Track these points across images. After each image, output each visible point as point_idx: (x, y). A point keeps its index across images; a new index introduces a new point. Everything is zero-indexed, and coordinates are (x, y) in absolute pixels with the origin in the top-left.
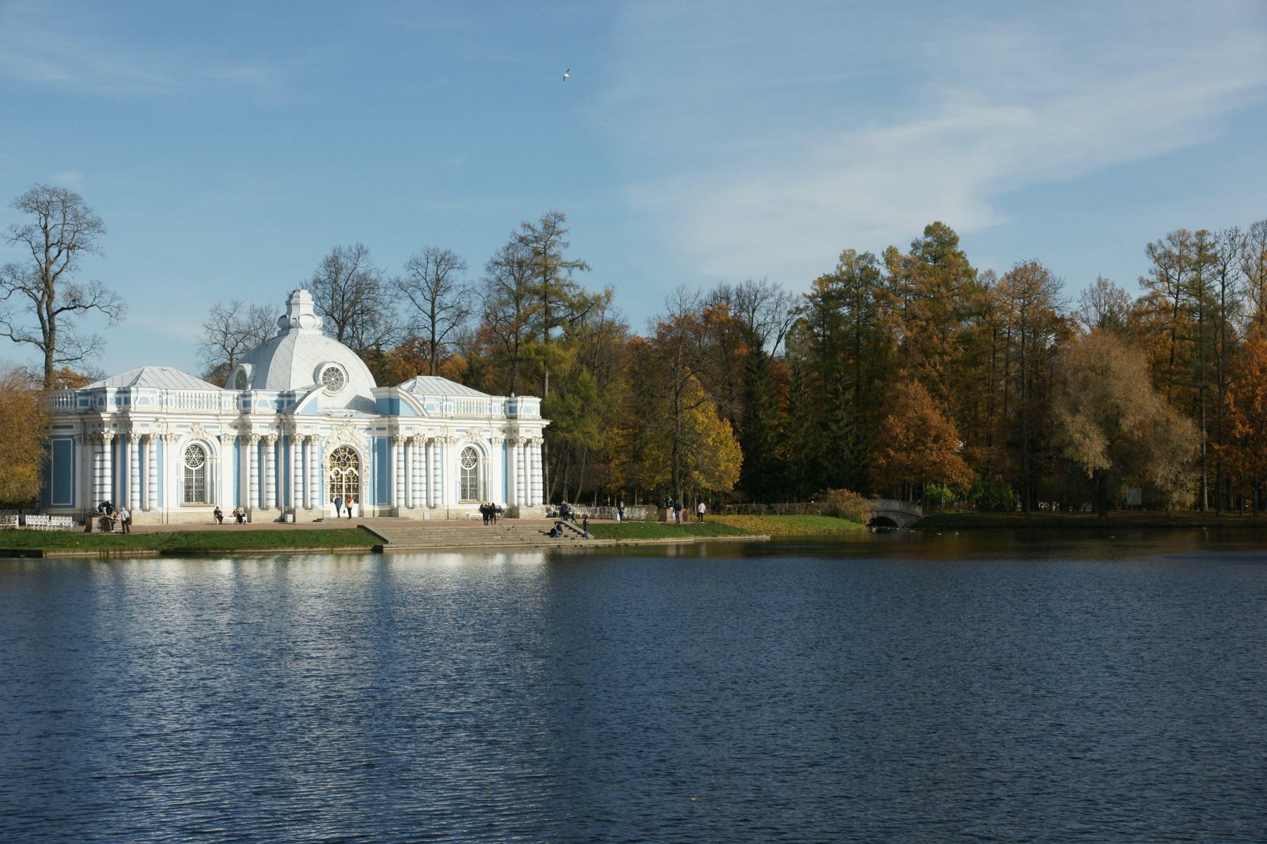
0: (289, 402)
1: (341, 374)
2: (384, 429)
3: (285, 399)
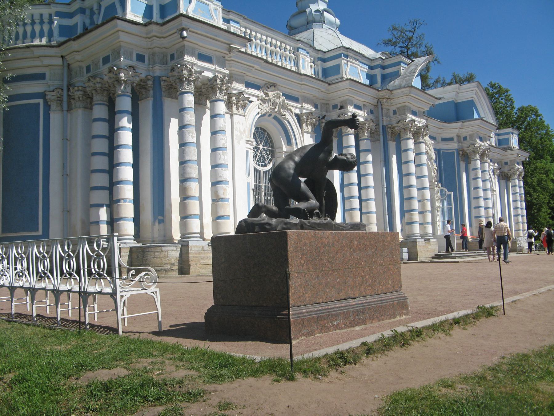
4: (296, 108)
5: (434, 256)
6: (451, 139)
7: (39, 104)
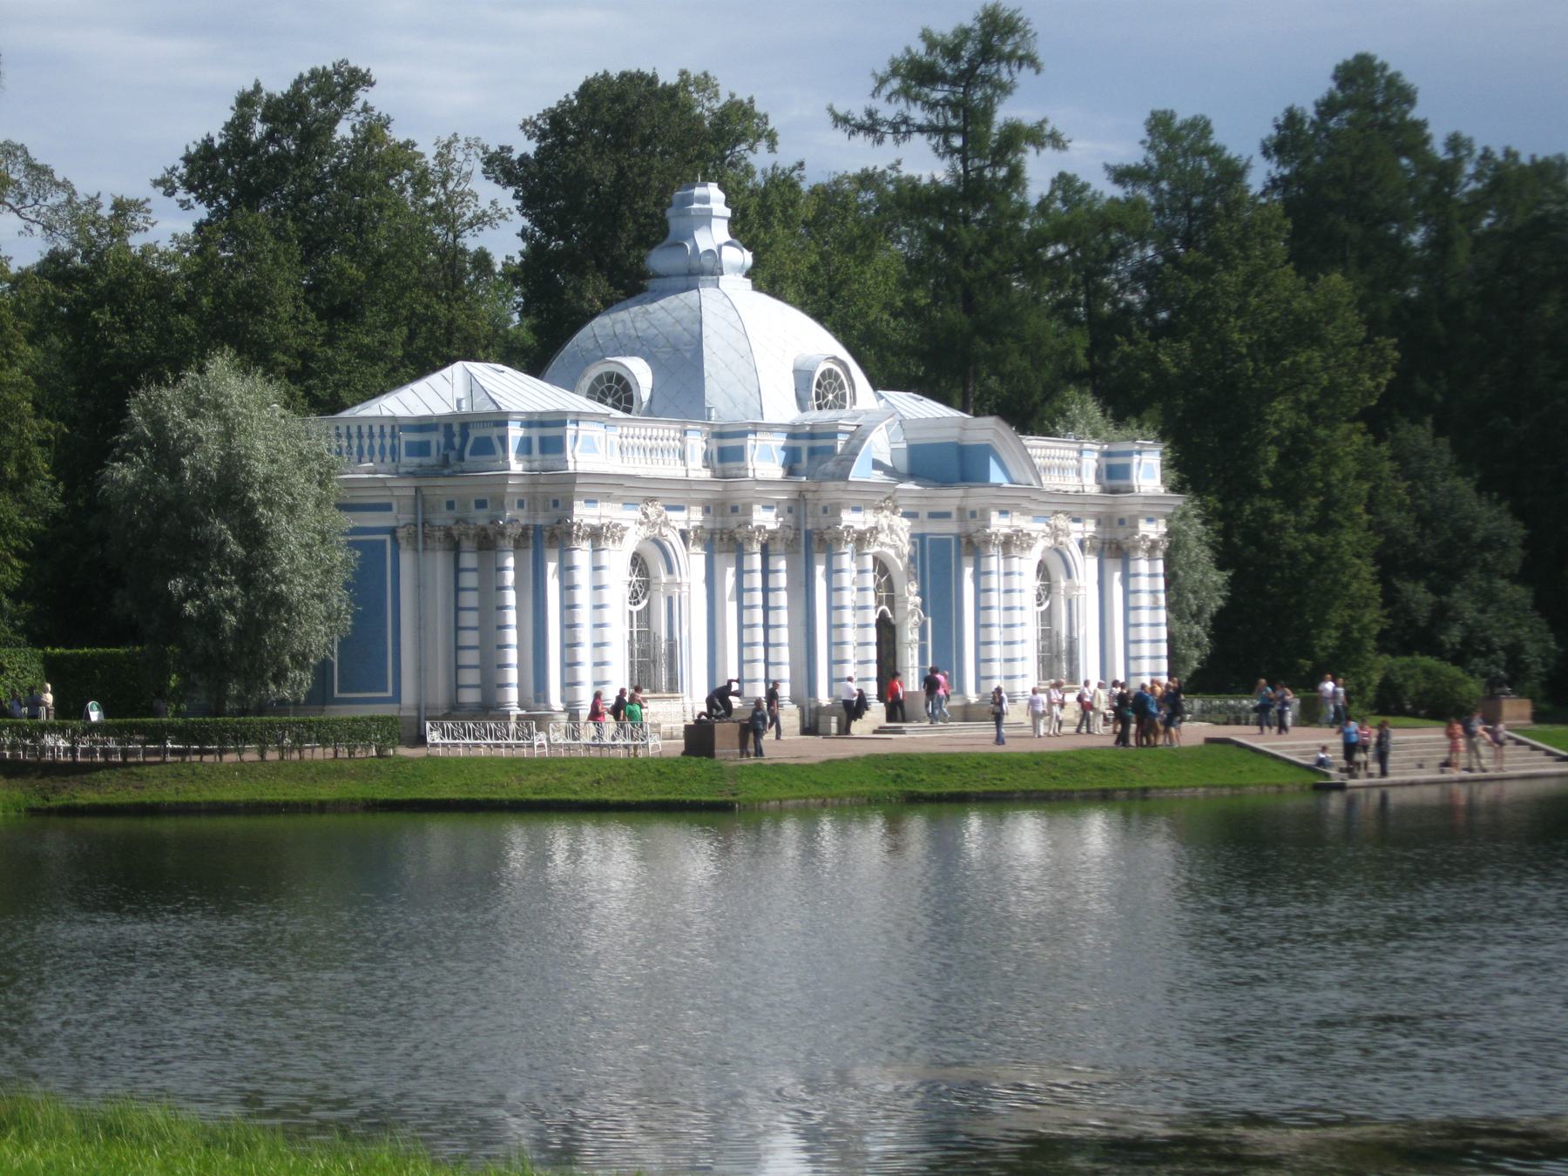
0: (813, 452)
1: (841, 387)
2: (946, 515)
3: (804, 445)
4: (679, 519)
5: (876, 728)
6: (946, 515)
7: (384, 542)
